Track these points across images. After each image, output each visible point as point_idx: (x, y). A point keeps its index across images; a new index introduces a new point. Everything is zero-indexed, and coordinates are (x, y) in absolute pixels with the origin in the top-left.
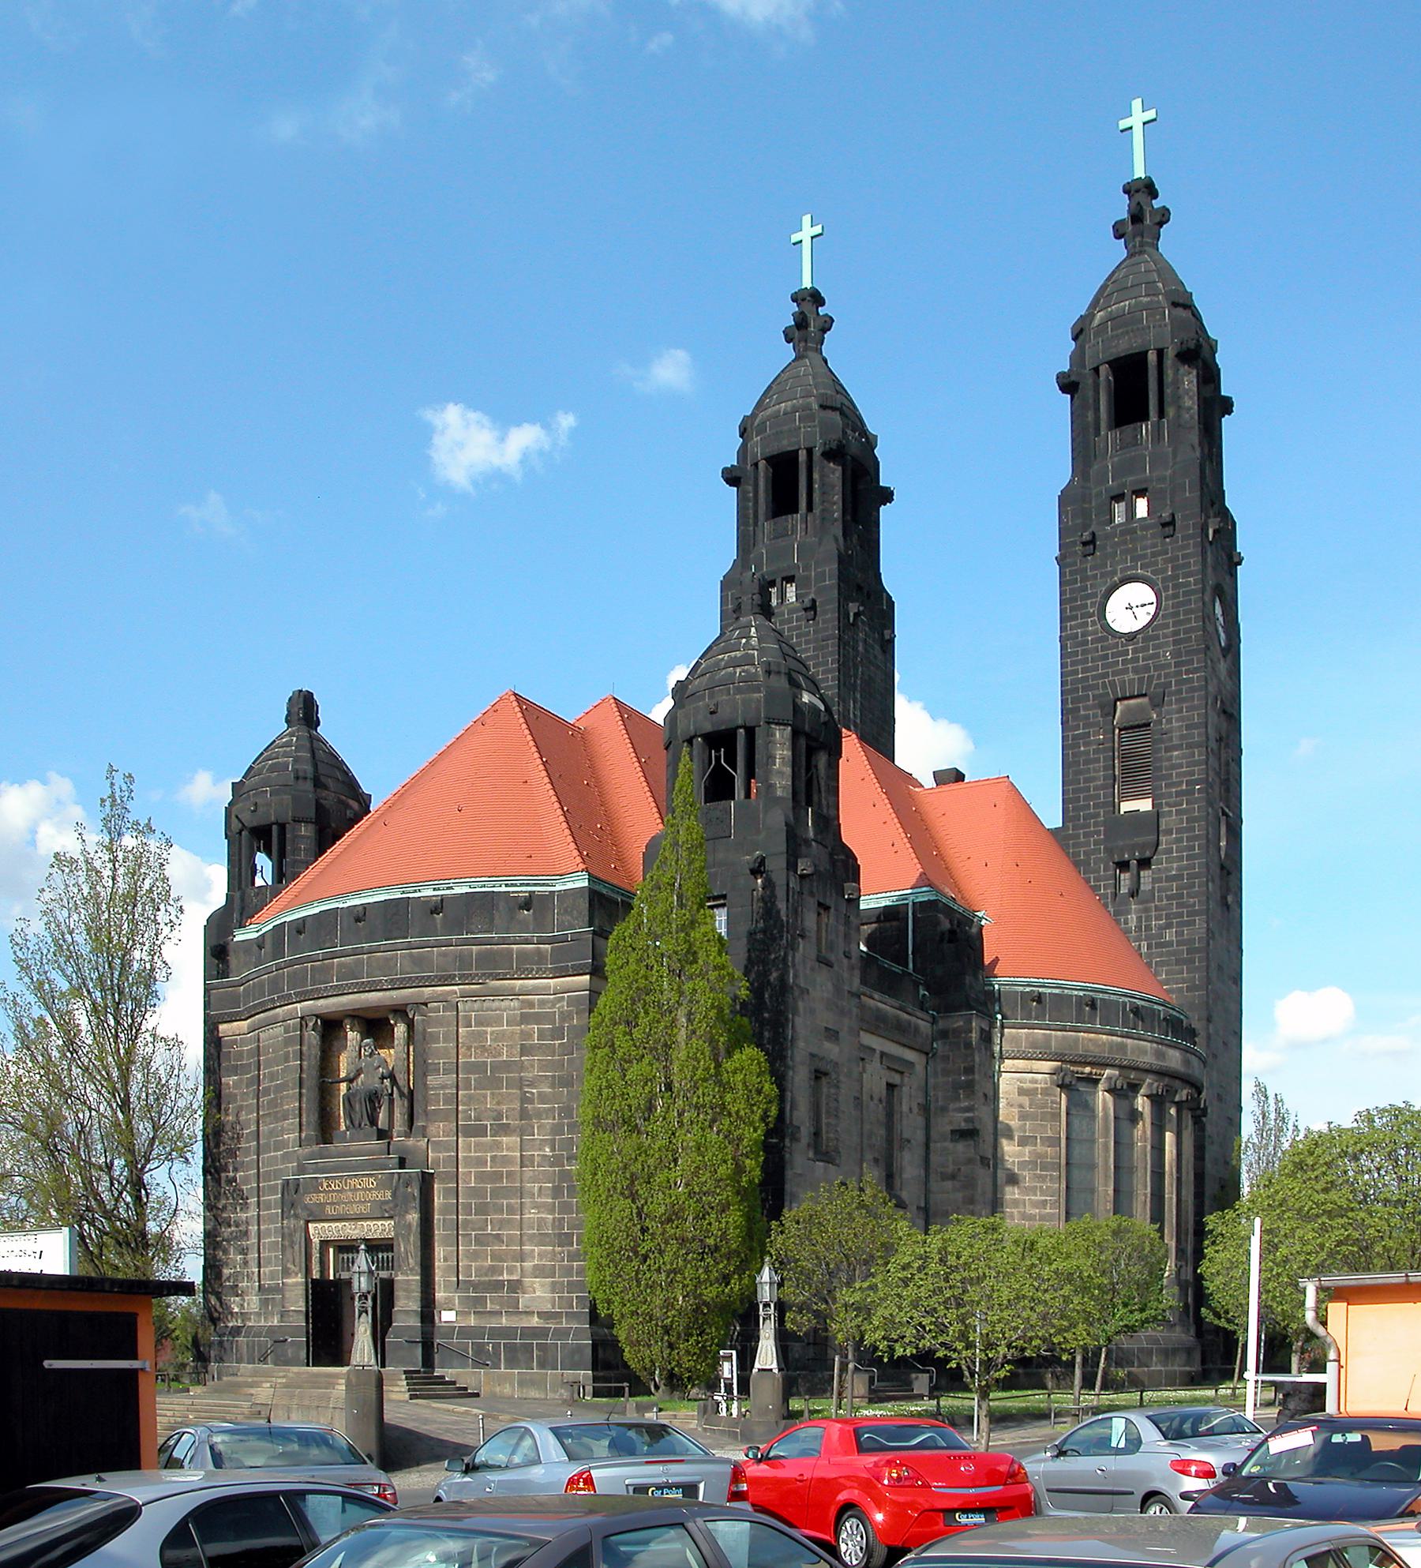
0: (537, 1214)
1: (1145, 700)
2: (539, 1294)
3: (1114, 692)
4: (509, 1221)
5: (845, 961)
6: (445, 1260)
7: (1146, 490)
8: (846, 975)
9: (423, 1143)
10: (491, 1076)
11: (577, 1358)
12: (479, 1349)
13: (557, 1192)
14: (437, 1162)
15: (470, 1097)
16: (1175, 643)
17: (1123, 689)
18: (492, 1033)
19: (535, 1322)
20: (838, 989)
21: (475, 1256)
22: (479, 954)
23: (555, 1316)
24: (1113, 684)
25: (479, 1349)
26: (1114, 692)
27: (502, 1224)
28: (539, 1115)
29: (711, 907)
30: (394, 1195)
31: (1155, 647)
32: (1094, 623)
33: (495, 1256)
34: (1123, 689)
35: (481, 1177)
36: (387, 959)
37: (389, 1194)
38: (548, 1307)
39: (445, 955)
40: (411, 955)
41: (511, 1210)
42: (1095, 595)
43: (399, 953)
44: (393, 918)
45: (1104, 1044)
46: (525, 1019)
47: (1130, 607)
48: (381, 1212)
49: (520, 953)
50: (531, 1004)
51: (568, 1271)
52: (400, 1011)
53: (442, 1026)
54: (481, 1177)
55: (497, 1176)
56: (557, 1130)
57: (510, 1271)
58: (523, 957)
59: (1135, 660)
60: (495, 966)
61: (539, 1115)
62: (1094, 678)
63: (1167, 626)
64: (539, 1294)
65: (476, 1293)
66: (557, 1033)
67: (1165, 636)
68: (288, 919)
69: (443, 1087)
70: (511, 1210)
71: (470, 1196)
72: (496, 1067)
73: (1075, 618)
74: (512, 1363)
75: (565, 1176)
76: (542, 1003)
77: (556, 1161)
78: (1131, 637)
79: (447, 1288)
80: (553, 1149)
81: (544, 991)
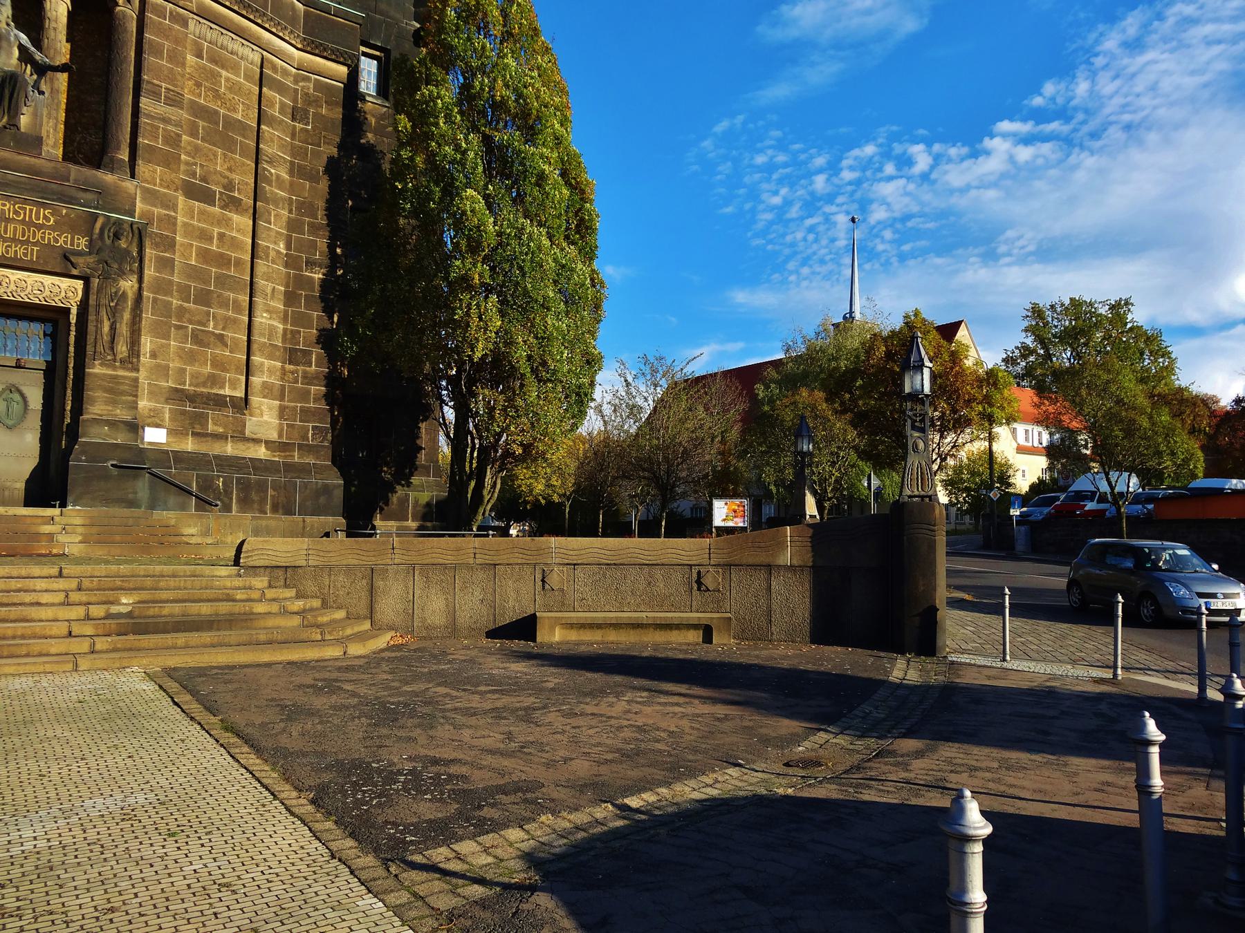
0: (270, 320)
2: (265, 419)
4: (235, 321)
6: (154, 355)
9: (129, 185)
10: (221, 132)
11: (322, 500)
12: (207, 484)
13: (290, 298)
14: (149, 217)
15: (197, 149)
18: (227, 80)
19: (261, 452)
21: (191, 357)
23: (282, 447)
25: (207, 484)
27: (228, 323)
28: (276, 201)
29: (365, 54)
30: (91, 243)
33: (218, 363)
35: (204, 255)
37: (82, 243)
38: (274, 436)
41: (237, 307)
48: (64, 265)
50: (274, 68)
51: (304, 396)
54: (204, 255)
55: (223, 261)
56: (293, 226)
57: (233, 385)
61: (276, 201)
64: (265, 419)
65: (194, 406)
69: (166, 120)
70: (237, 307)
71: (189, 277)
72: (230, 123)
74: (245, 503)
75: (300, 282)
76: (285, 73)
77: (290, 262)
79: (153, 394)
80: (288, 247)
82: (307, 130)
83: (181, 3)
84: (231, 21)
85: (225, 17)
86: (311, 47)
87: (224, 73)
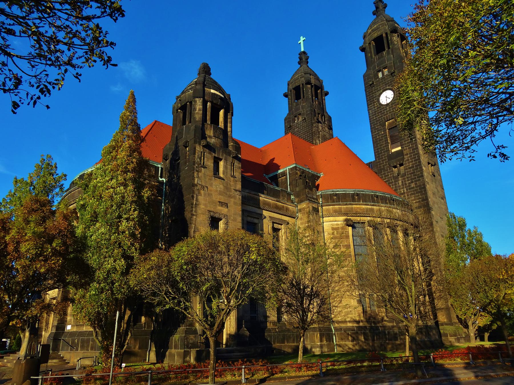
1: (393, 120)
3: (385, 120)
17: (387, 118)
26: (385, 120)
34: (387, 118)
42: (376, 97)
45: (364, 209)
47: (386, 97)
59: (390, 110)
78: (387, 104)
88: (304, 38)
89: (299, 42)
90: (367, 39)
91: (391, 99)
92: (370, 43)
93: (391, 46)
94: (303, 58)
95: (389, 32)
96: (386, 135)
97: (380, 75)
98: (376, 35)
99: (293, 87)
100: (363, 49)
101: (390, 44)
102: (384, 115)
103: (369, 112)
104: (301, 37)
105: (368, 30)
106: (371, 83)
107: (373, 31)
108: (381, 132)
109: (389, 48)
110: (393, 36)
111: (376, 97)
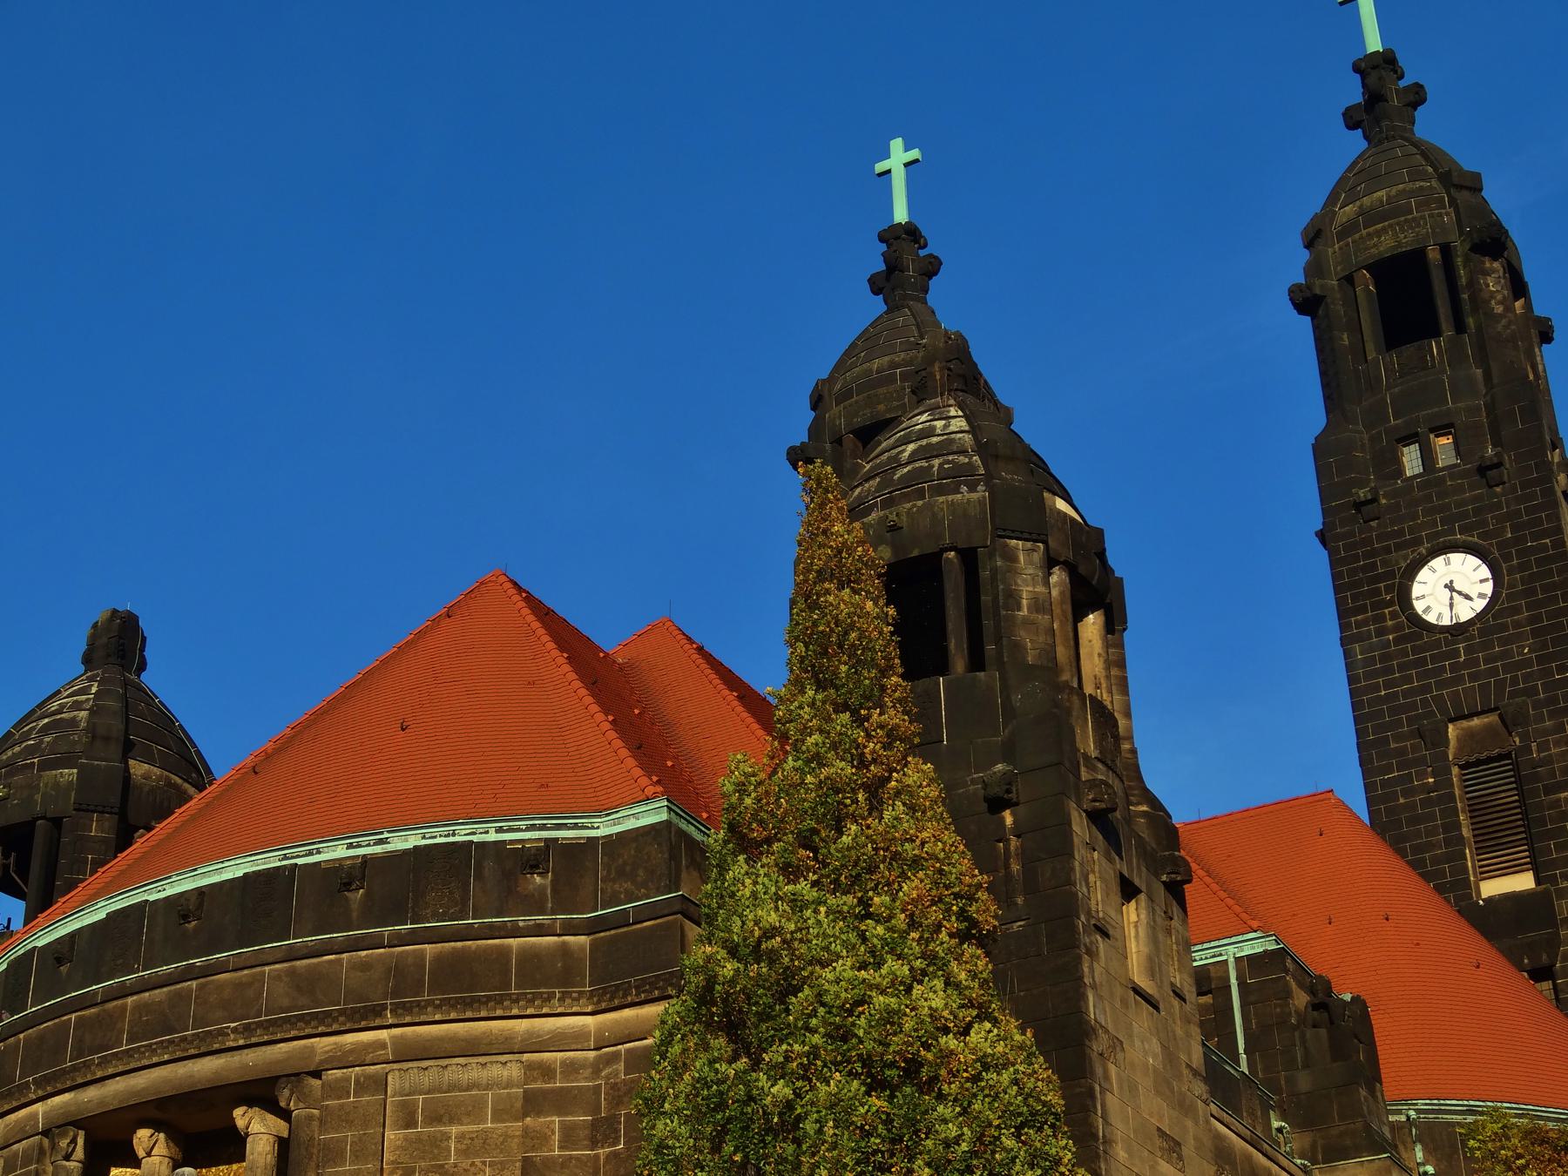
1: (1493, 718)
3: (1443, 709)
5: (1176, 1002)
7: (1452, 425)
8: (1179, 1032)
16: (1535, 633)
18: (461, 1137)
20: (1170, 1056)
22: (438, 959)
24: (1439, 700)
26: (1443, 709)
31: (1504, 642)
32: (1394, 615)
36: (239, 986)
39: (365, 966)
40: (292, 973)
42: (1391, 575)
43: (263, 966)
44: (261, 905)
46: (533, 1103)
47: (1452, 588)
49: (528, 956)
50: (546, 1071)
52: (261, 1092)
53: (350, 1123)
58: (530, 959)
60: (470, 985)
62: (1406, 694)
63: (1516, 610)
66: (602, 1131)
67: (1517, 625)
68: (40, 943)
73: (1363, 610)
76: (571, 1068)
78: (1458, 630)
81: (572, 1040)
82: (616, 1154)
83: (368, 1059)
84: (453, 1039)
85: (440, 1039)
86: (609, 997)
87: (454, 1130)
88: (915, 154)
89: (880, 167)
90: (1332, 250)
91: (1480, 605)
92: (1349, 280)
93: (1471, 321)
94: (904, 264)
95: (1460, 247)
96: (1452, 797)
97: (1411, 460)
98: (1386, 243)
99: (858, 421)
100: (1306, 302)
101: (1467, 307)
102: (1441, 685)
103: (1347, 654)
104: (897, 145)
105: (1332, 198)
106: (1363, 494)
107: (1371, 217)
108: (1424, 775)
109: (1460, 327)
110: (1486, 273)
111: (1391, 575)
